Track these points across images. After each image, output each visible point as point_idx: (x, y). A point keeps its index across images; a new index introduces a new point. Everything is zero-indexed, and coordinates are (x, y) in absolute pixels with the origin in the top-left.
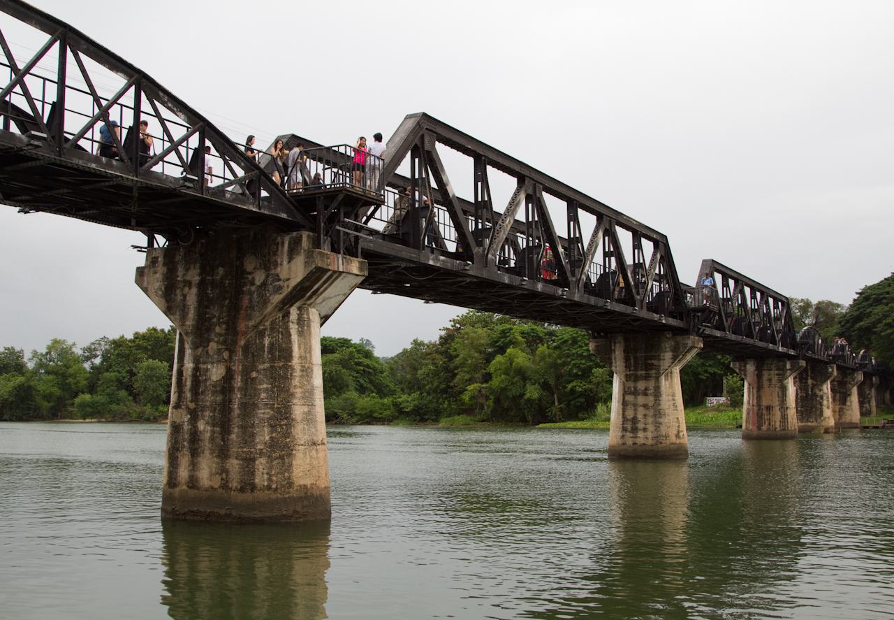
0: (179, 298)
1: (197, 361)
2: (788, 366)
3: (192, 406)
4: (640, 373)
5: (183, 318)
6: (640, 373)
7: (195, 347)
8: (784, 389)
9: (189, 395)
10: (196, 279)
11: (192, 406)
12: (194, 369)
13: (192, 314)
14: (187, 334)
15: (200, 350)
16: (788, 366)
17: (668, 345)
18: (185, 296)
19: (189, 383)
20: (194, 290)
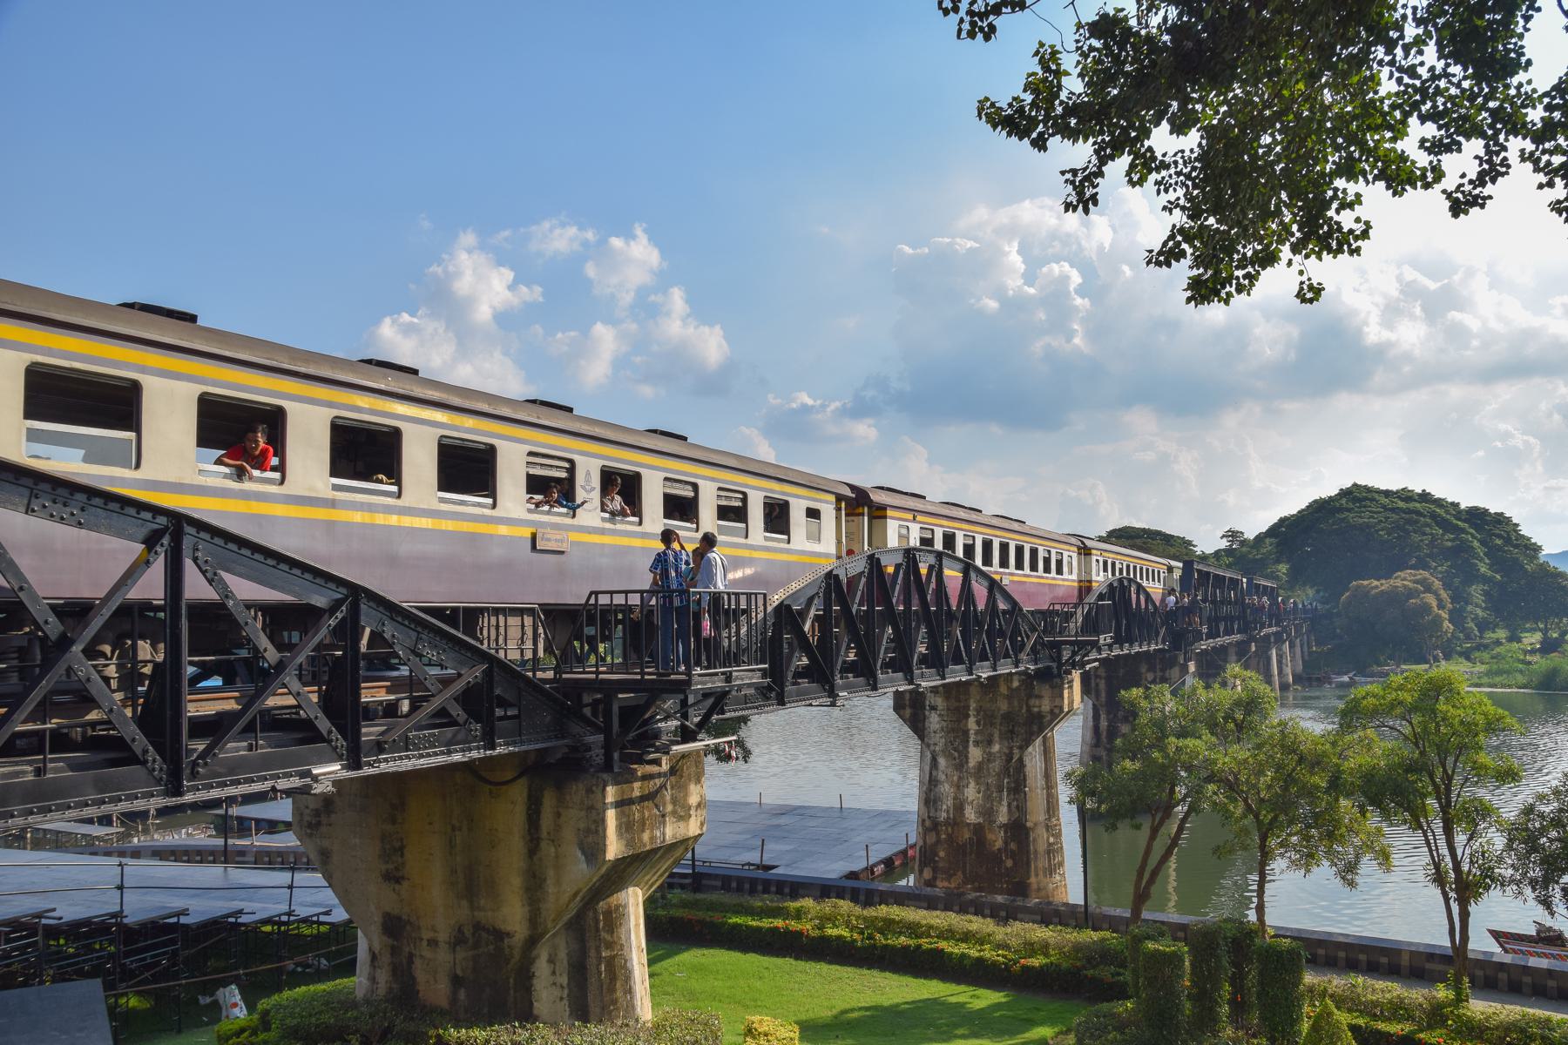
0: (1093, 685)
1: (1108, 720)
2: (1272, 640)
3: (1108, 746)
4: (1210, 672)
5: (1098, 697)
6: (1210, 672)
7: (1108, 713)
8: (1269, 659)
9: (1105, 740)
10: (1103, 674)
11: (1108, 746)
12: (1109, 726)
13: (1103, 694)
14: (1101, 706)
15: (1111, 716)
16: (1272, 640)
17: (1232, 651)
18: (1097, 685)
19: (1105, 733)
20: (1103, 681)
